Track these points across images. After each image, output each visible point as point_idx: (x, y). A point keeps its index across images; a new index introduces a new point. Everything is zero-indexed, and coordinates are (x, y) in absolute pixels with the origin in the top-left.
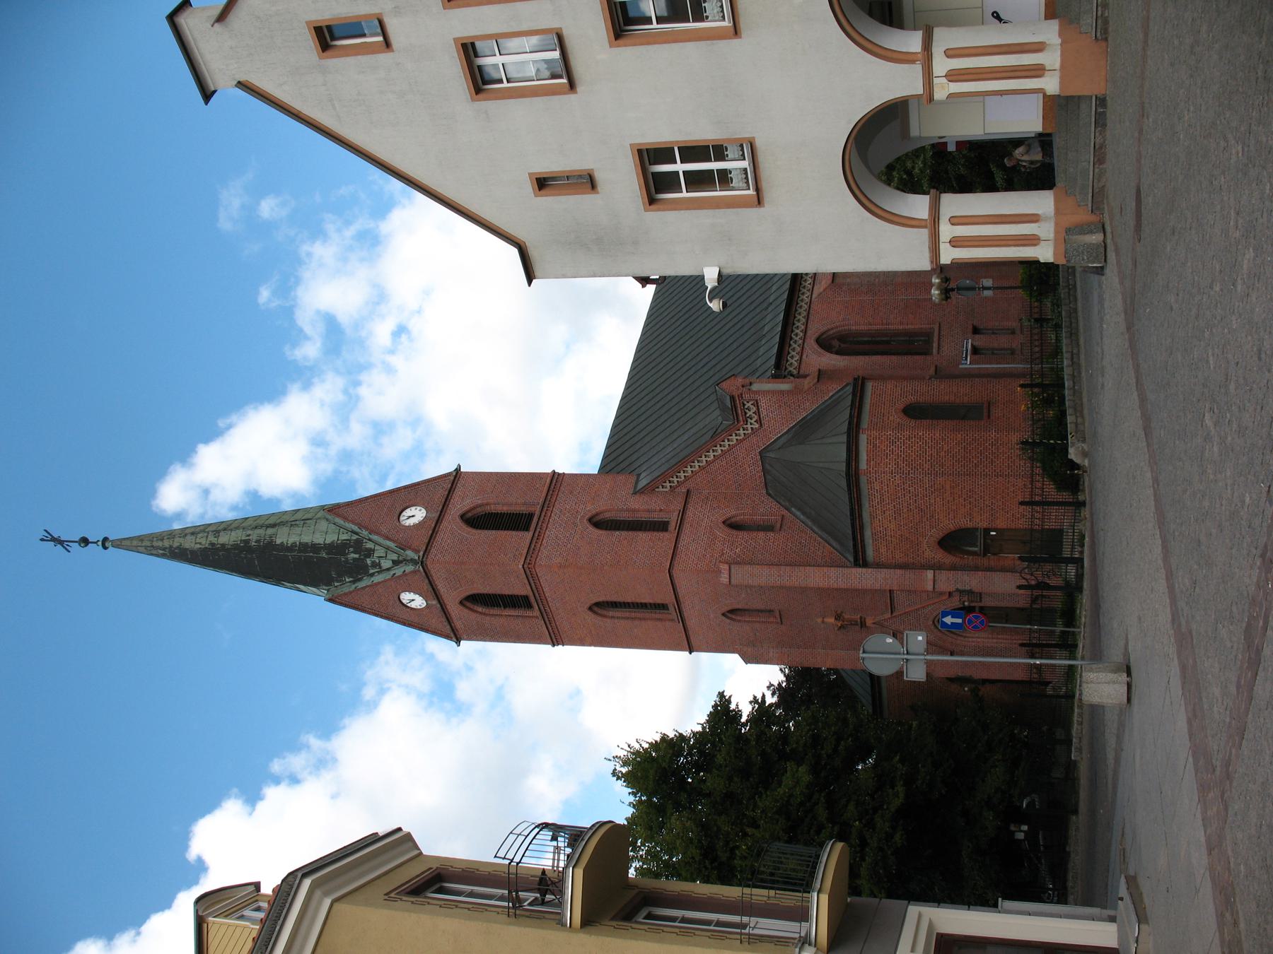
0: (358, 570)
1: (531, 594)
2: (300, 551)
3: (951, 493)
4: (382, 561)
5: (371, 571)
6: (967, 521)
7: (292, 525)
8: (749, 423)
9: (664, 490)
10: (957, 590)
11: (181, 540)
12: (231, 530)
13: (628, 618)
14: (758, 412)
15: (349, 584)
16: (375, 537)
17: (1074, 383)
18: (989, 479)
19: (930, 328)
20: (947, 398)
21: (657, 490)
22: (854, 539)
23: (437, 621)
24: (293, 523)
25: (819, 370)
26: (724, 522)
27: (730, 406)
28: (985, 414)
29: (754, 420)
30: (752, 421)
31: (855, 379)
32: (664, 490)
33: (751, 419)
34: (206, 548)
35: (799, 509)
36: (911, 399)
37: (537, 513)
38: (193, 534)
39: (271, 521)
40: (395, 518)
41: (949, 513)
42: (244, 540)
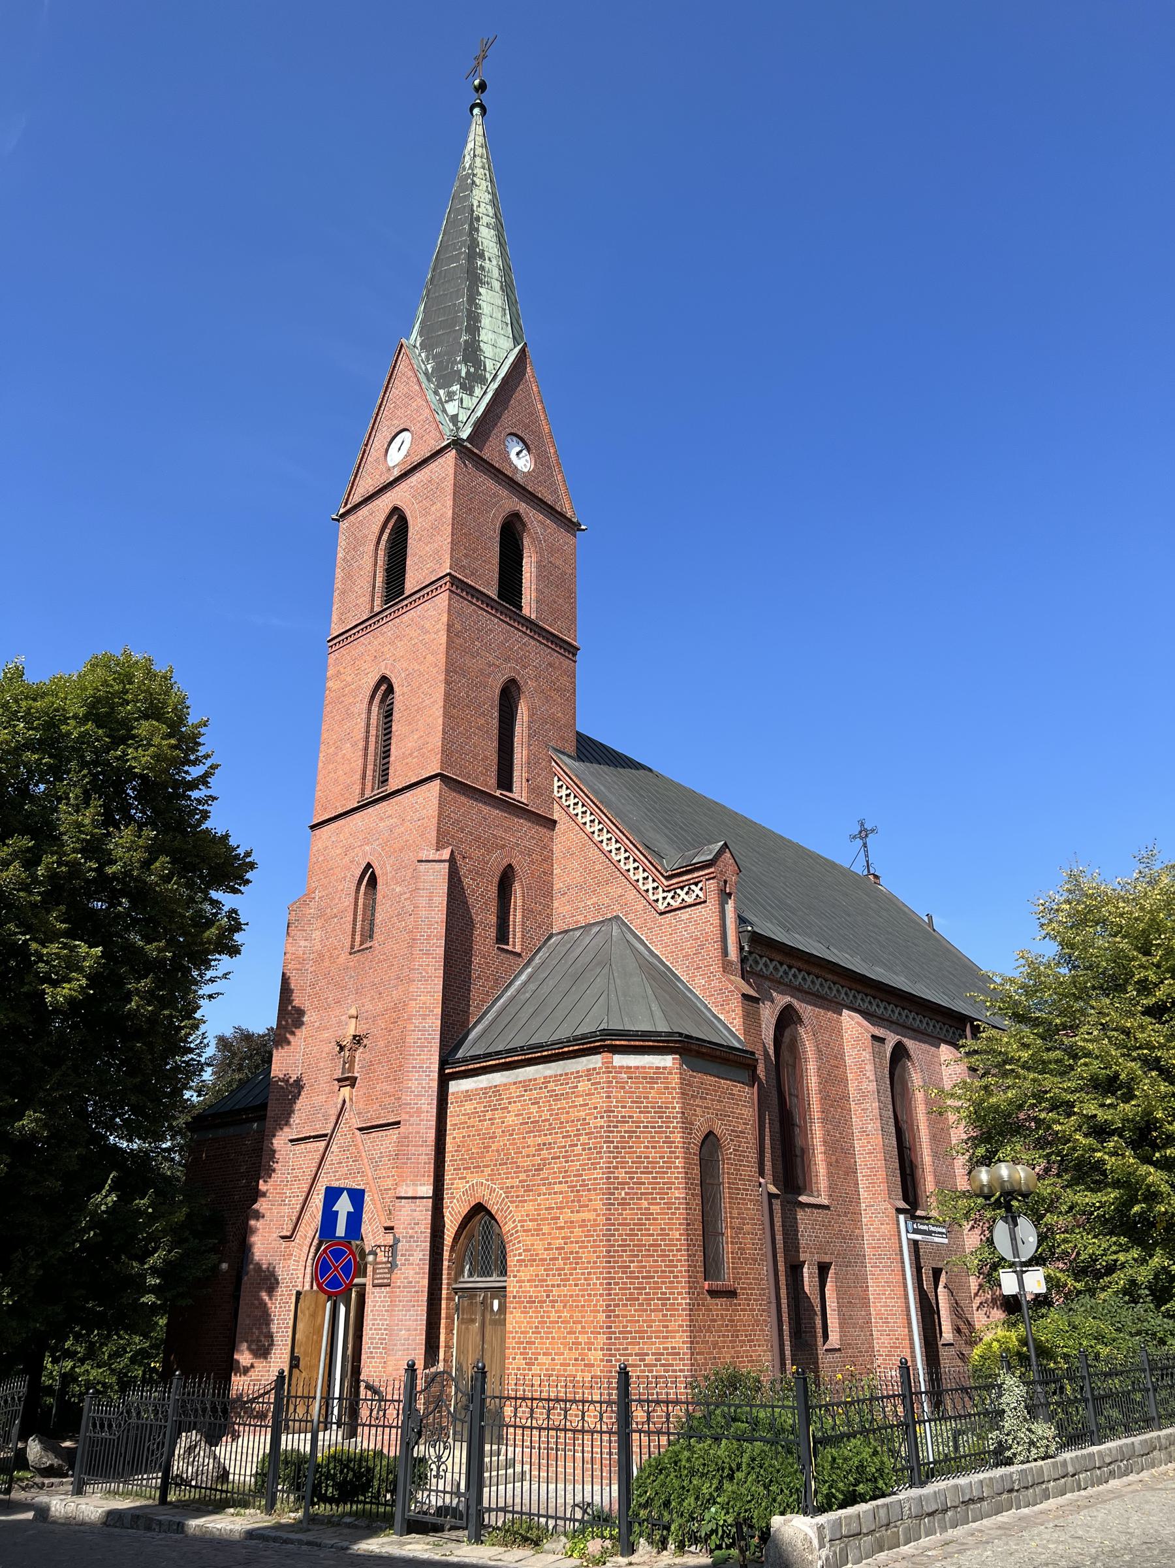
1: (407, 593)
2: (469, 312)
3: (572, 1222)
5: (441, 392)
6: (520, 1255)
9: (556, 789)
10: (397, 1241)
13: (368, 732)
18: (601, 1295)
19: (818, 1191)
21: (556, 779)
22: (488, 1056)
24: (507, 312)
26: (510, 865)
27: (694, 861)
29: (672, 902)
30: (669, 900)
32: (556, 789)
33: (673, 897)
35: (530, 977)
36: (729, 1149)
40: (514, 430)
41: (536, 1220)
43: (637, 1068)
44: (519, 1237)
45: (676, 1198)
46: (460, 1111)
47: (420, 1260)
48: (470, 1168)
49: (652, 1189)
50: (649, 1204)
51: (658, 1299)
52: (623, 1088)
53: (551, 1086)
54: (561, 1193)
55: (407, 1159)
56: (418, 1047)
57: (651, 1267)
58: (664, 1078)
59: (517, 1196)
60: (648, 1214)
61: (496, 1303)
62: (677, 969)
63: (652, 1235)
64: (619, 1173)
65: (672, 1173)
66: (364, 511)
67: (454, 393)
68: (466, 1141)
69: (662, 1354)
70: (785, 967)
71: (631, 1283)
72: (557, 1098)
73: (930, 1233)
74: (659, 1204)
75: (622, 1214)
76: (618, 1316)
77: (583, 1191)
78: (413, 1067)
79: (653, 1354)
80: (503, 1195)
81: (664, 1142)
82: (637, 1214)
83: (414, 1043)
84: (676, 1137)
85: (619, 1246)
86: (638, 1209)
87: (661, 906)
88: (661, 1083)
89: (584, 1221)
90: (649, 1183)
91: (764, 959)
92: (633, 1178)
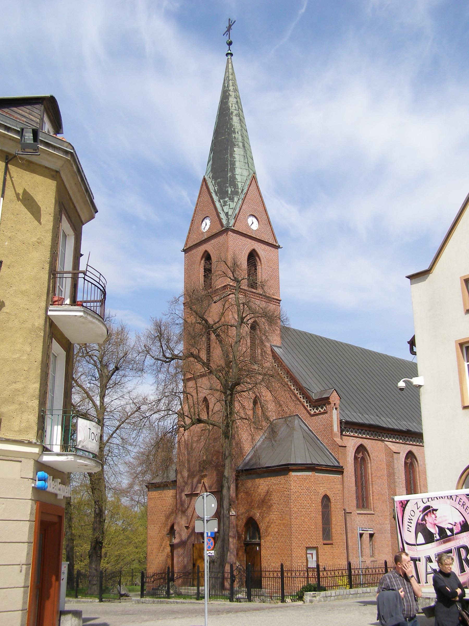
0: (222, 194)
4: (227, 207)
5: (221, 201)
7: (245, 156)
11: (233, 96)
12: (240, 123)
15: (214, 189)
16: (240, 202)
17: (353, 594)
20: (334, 519)
23: (195, 239)
24: (246, 157)
25: (346, 447)
28: (326, 542)
29: (316, 411)
31: (342, 467)
34: (230, 110)
36: (332, 500)
37: (257, 292)
38: (237, 102)
39: (246, 145)
42: (235, 130)
52: (295, 482)
54: (277, 515)
60: (304, 521)
61: (258, 548)
66: (194, 251)
67: (226, 202)
70: (360, 430)
72: (274, 485)
73: (367, 531)
76: (295, 552)
87: (312, 412)
89: (284, 523)
91: (351, 429)
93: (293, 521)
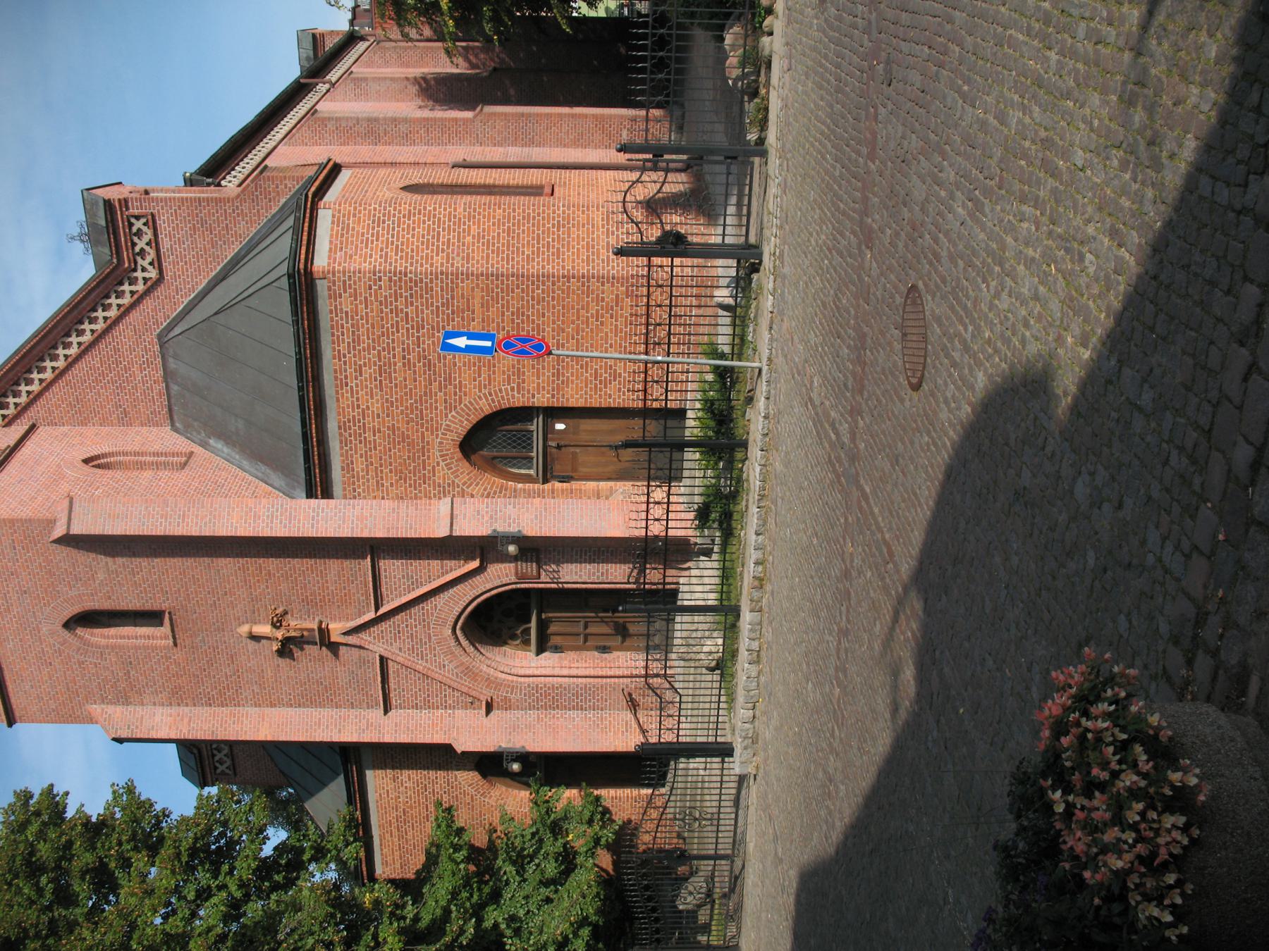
6: (513, 389)
8: (139, 268)
14: (155, 243)
29: (149, 259)
30: (145, 263)
41: (479, 368)
43: (331, 242)
44: (495, 391)
45: (465, 211)
46: (363, 477)
47: (514, 507)
48: (424, 461)
49: (454, 231)
50: (469, 235)
51: (558, 231)
52: (351, 257)
53: (343, 348)
55: (411, 528)
56: (290, 523)
57: (528, 236)
58: (344, 216)
59: (455, 394)
62: (226, 256)
63: (499, 234)
64: (437, 262)
65: (440, 213)
68: (396, 467)
69: (608, 229)
71: (543, 254)
74: (469, 226)
75: (478, 261)
77: (453, 306)
78: (313, 527)
79: (608, 237)
80: (453, 413)
81: (409, 219)
82: (478, 247)
83: (285, 527)
84: (405, 208)
85: (508, 264)
86: (473, 245)
87: (153, 274)
88: (349, 219)
90: (449, 234)
92: (443, 250)
93: (475, 268)
